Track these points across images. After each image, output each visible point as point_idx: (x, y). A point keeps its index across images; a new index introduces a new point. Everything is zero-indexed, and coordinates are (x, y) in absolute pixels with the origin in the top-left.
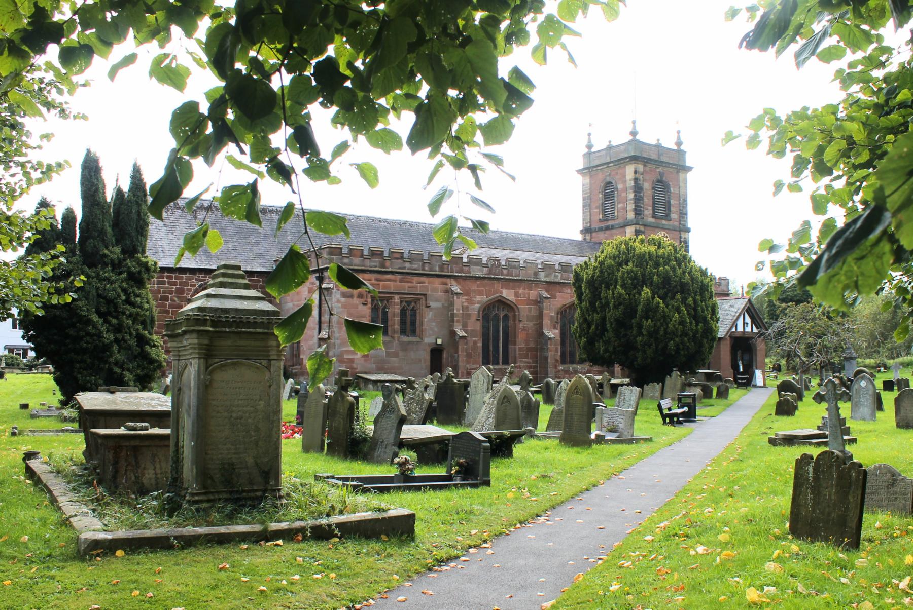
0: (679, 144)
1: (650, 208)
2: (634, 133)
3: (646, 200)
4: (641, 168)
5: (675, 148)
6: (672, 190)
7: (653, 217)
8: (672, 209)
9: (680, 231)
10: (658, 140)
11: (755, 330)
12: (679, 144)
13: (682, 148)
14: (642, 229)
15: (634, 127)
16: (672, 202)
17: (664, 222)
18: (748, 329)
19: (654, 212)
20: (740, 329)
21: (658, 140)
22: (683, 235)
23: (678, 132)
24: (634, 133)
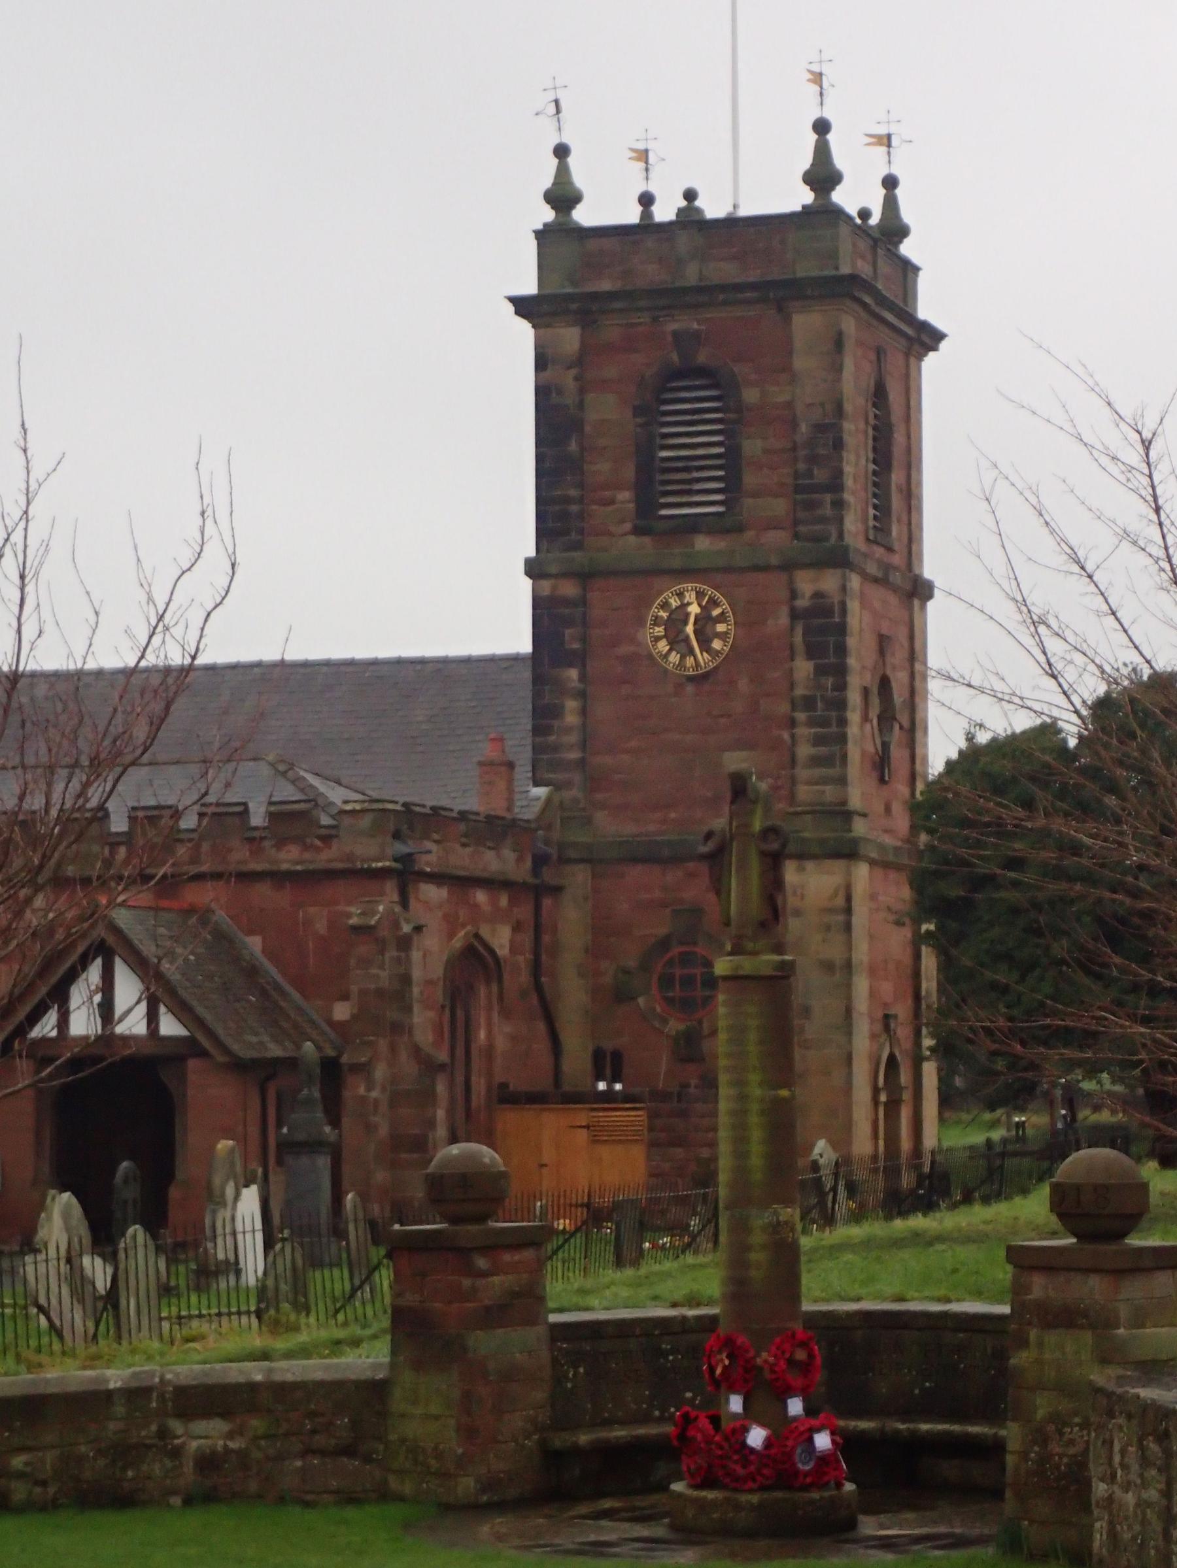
0: (823, 176)
1: (625, 496)
2: (562, 197)
3: (601, 468)
4: (570, 338)
5: (806, 196)
6: (750, 395)
7: (638, 531)
8: (750, 479)
9: (788, 566)
10: (690, 195)
11: (169, 1026)
12: (823, 176)
13: (838, 196)
14: (569, 589)
15: (563, 172)
16: (752, 447)
17: (702, 543)
18: (134, 1024)
19: (646, 507)
20: (83, 1023)
21: (690, 195)
22: (807, 584)
23: (822, 127)
24: (562, 197)
